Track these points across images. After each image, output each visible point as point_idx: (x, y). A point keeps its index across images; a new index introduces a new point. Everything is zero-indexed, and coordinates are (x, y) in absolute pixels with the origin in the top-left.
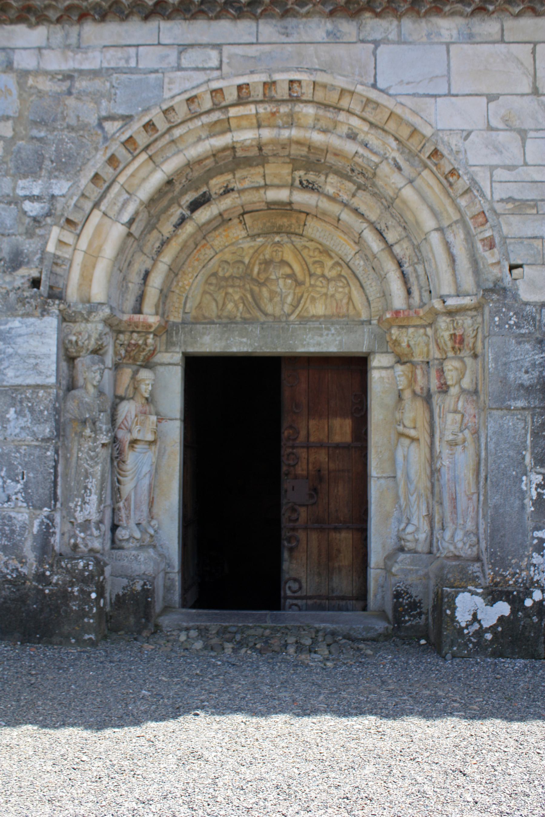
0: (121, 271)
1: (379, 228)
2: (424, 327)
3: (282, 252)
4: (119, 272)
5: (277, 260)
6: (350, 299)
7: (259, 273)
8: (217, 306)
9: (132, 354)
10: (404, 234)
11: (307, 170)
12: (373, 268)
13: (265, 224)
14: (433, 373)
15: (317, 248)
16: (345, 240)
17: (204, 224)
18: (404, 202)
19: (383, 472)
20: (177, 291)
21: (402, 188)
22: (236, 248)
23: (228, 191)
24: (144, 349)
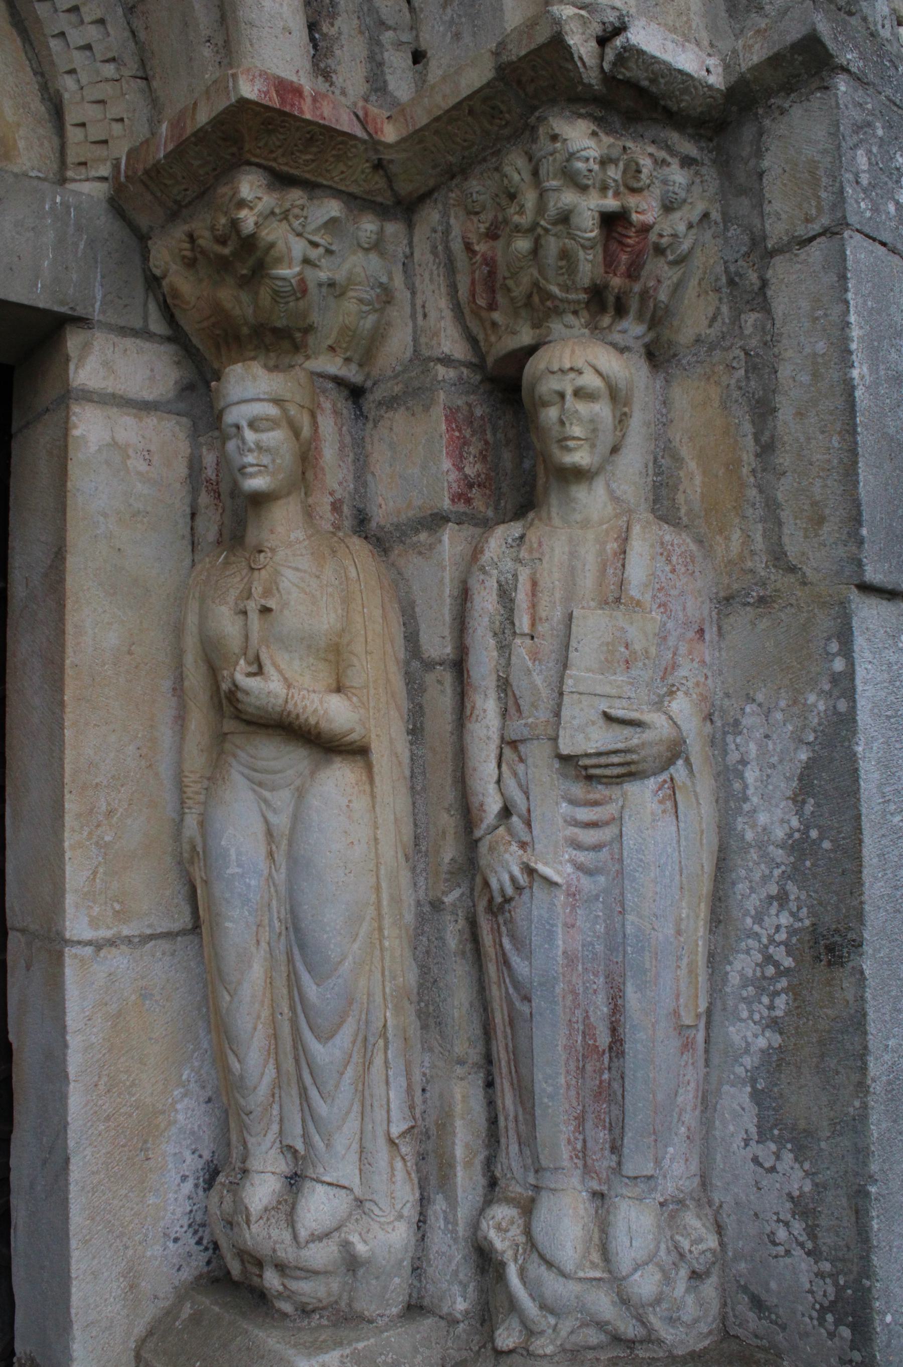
2: (383, 212)
19: (121, 916)
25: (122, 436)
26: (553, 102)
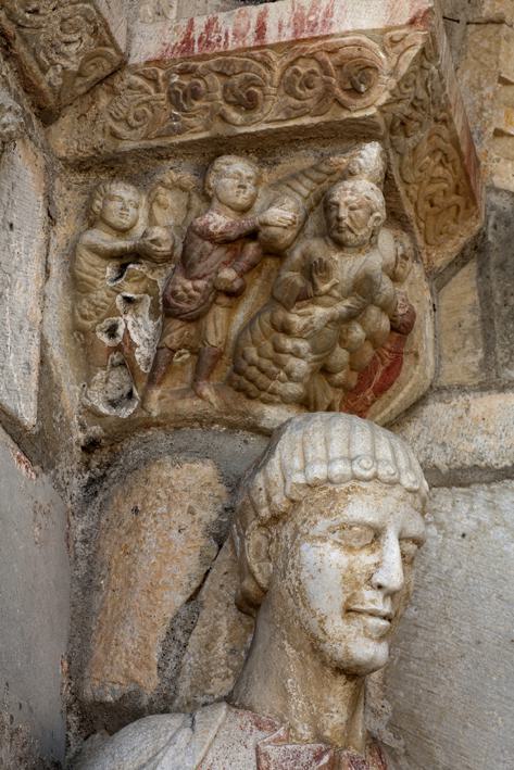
9: (222, 326)
24: (314, 270)
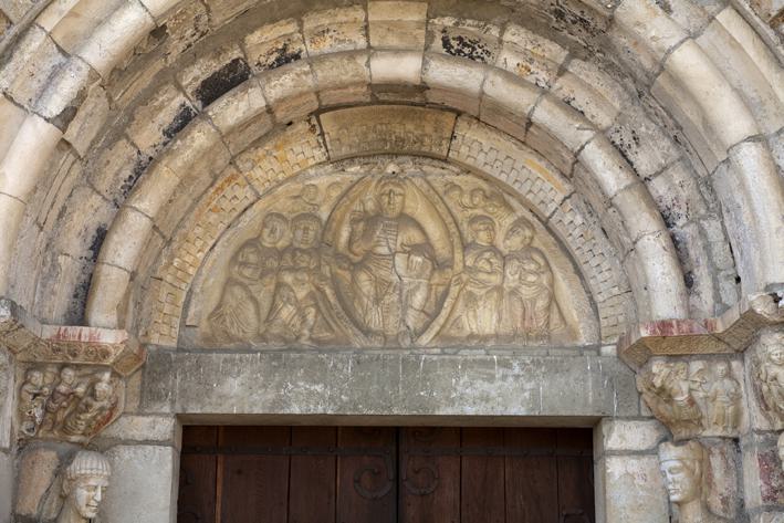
0: (41, 229)
1: (618, 142)
2: (727, 358)
3: (403, 195)
4: (36, 228)
5: (393, 214)
6: (553, 298)
7: (350, 242)
8: (258, 313)
10: (674, 154)
11: (461, 16)
12: (605, 232)
13: (365, 134)
14: (751, 466)
15: (480, 189)
16: (541, 170)
17: (232, 131)
18: (677, 81)
20: (169, 278)
21: (675, 47)
22: (301, 186)
23: (285, 58)
24: (88, 406)
25: (630, 471)
26: (764, 327)
